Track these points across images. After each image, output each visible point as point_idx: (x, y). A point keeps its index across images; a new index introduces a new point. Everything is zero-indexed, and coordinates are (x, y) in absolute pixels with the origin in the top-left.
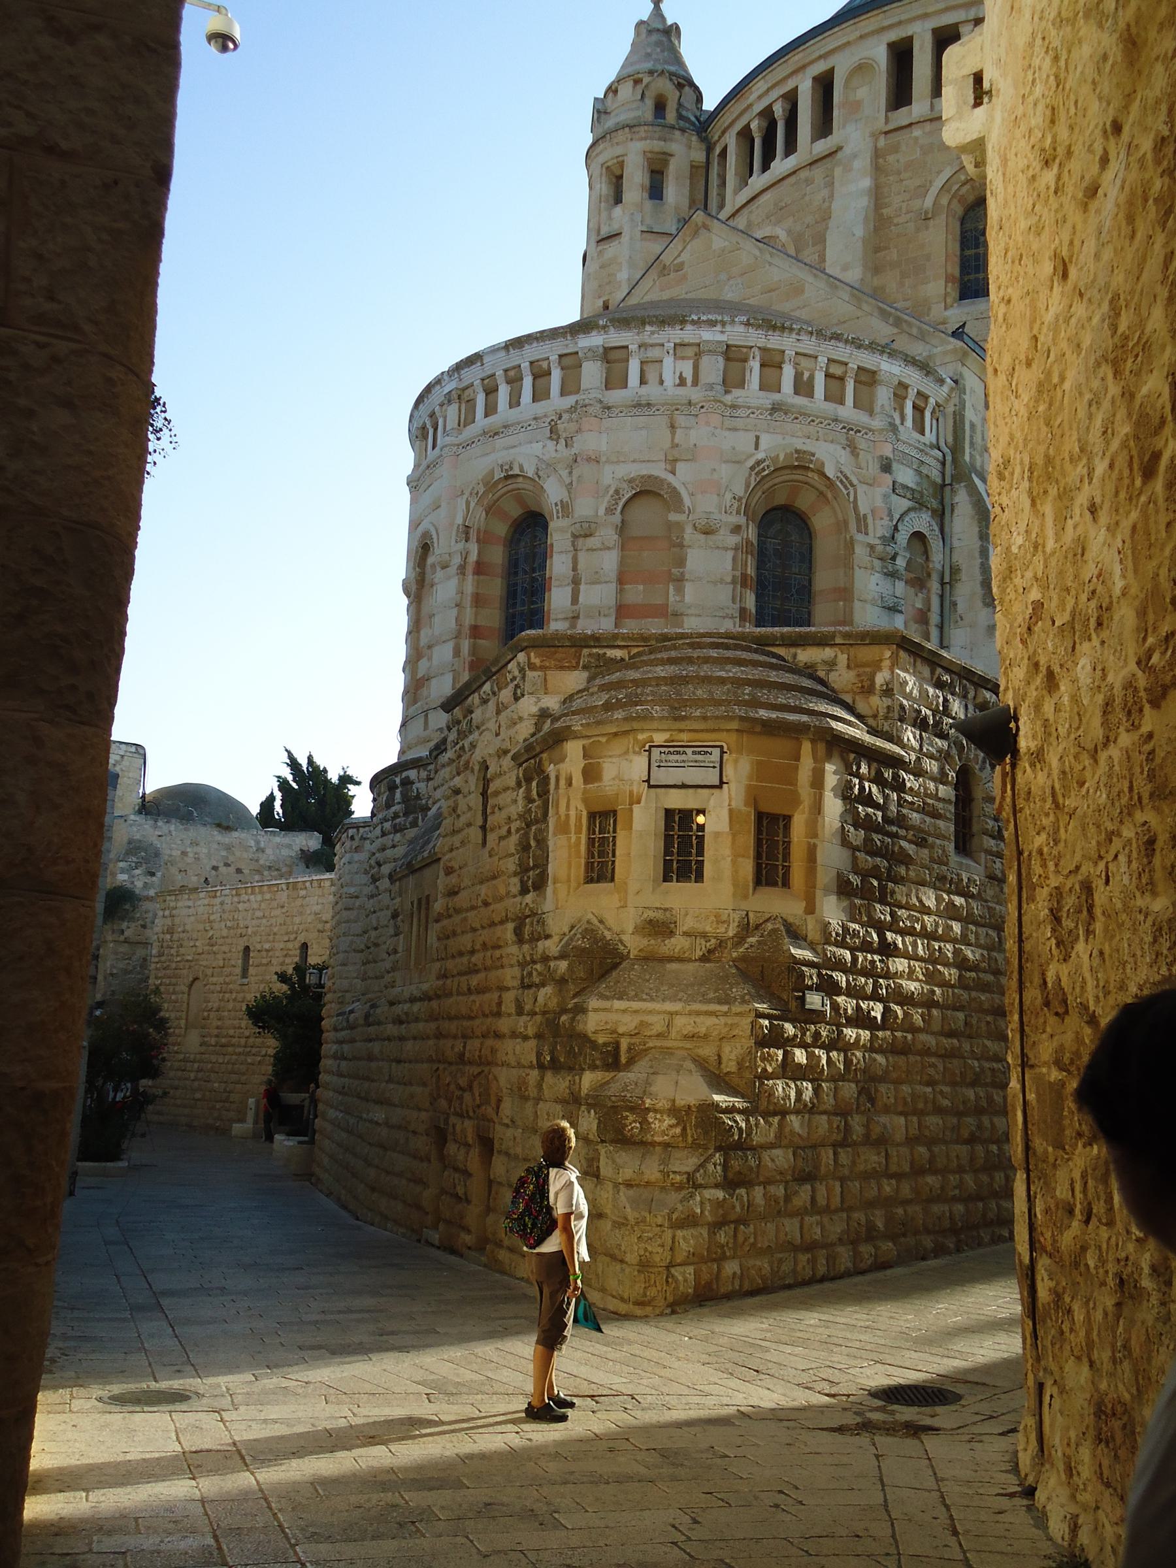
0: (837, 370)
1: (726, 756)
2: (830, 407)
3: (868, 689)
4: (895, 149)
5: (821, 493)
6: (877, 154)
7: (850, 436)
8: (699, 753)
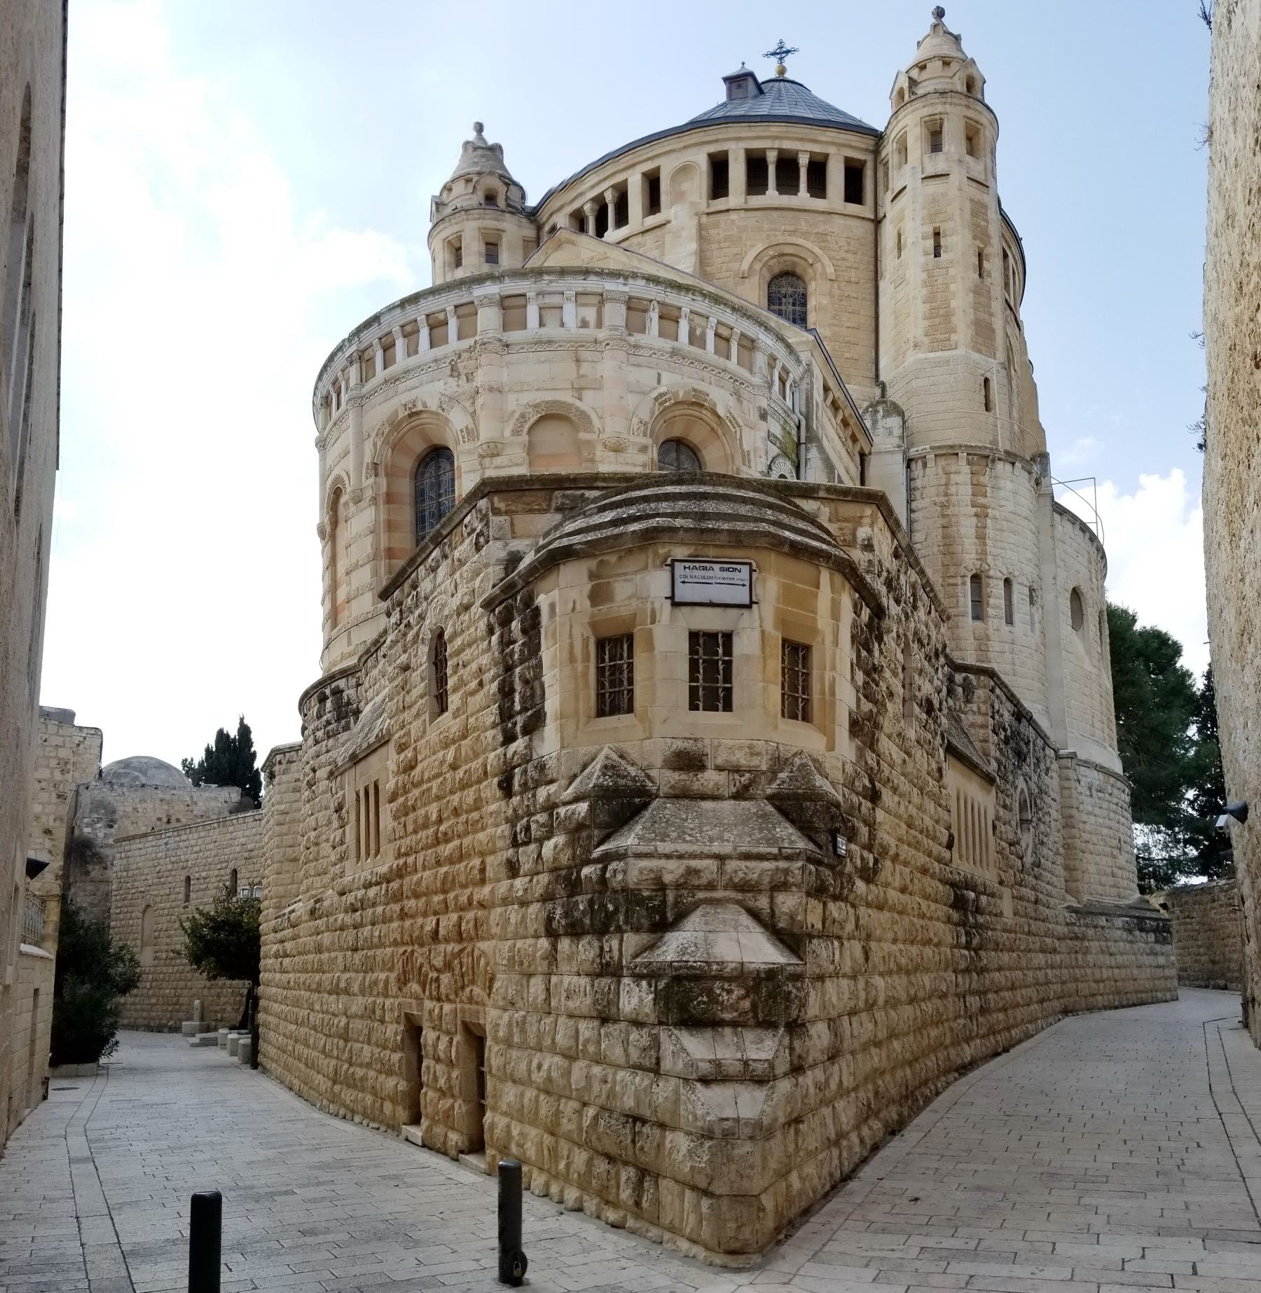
0: (725, 332)
1: (755, 575)
2: (721, 361)
3: (852, 543)
4: (717, 226)
5: (713, 429)
6: (701, 227)
7: (738, 388)
8: (728, 570)
